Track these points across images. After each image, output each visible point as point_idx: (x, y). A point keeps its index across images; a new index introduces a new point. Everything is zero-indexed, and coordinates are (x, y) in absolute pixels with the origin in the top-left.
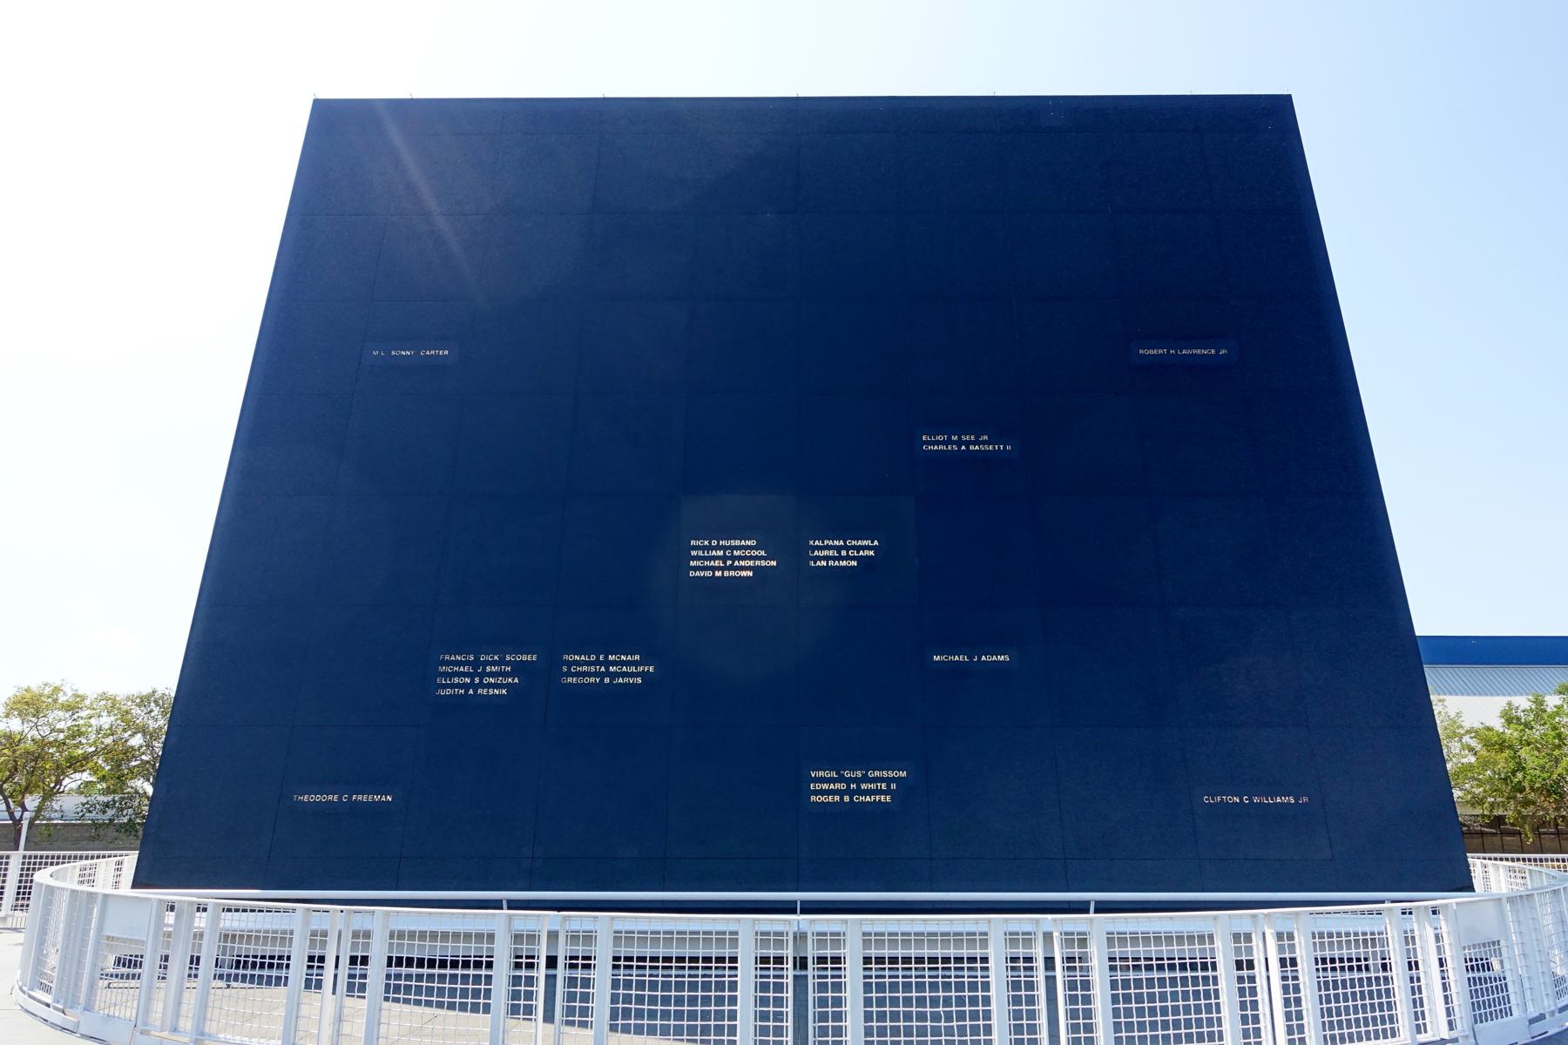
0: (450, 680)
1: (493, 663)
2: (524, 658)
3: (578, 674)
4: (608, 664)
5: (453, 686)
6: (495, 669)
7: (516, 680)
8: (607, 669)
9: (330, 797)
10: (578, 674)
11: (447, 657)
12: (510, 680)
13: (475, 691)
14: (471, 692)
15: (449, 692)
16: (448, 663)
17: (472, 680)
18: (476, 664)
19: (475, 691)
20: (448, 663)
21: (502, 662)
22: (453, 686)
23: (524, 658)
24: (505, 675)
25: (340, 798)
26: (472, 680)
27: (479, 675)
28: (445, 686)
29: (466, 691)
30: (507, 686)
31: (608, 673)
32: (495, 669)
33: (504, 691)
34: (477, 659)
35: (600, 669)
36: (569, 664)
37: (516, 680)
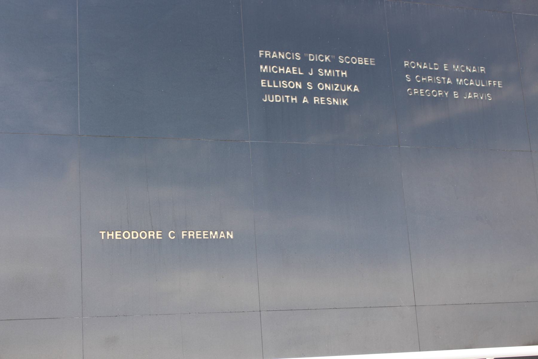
0: (277, 84)
1: (325, 66)
2: (360, 61)
3: (424, 85)
4: (454, 76)
5: (282, 92)
6: (329, 73)
7: (356, 89)
8: (454, 81)
9: (151, 234)
10: (424, 85)
11: (267, 54)
12: (349, 88)
13: (311, 100)
14: (305, 100)
15: (276, 99)
16: (269, 62)
17: (304, 86)
18: (304, 65)
19: (311, 100)
20: (269, 62)
21: (334, 65)
22: (282, 92)
23: (360, 61)
24: (343, 81)
25: (164, 235)
26: (304, 86)
27: (310, 79)
28: (272, 92)
29: (300, 99)
30: (349, 95)
31: (454, 87)
32: (329, 73)
33: (344, 102)
34: (305, 59)
35: (446, 80)
36: (413, 72)
37: (356, 89)
